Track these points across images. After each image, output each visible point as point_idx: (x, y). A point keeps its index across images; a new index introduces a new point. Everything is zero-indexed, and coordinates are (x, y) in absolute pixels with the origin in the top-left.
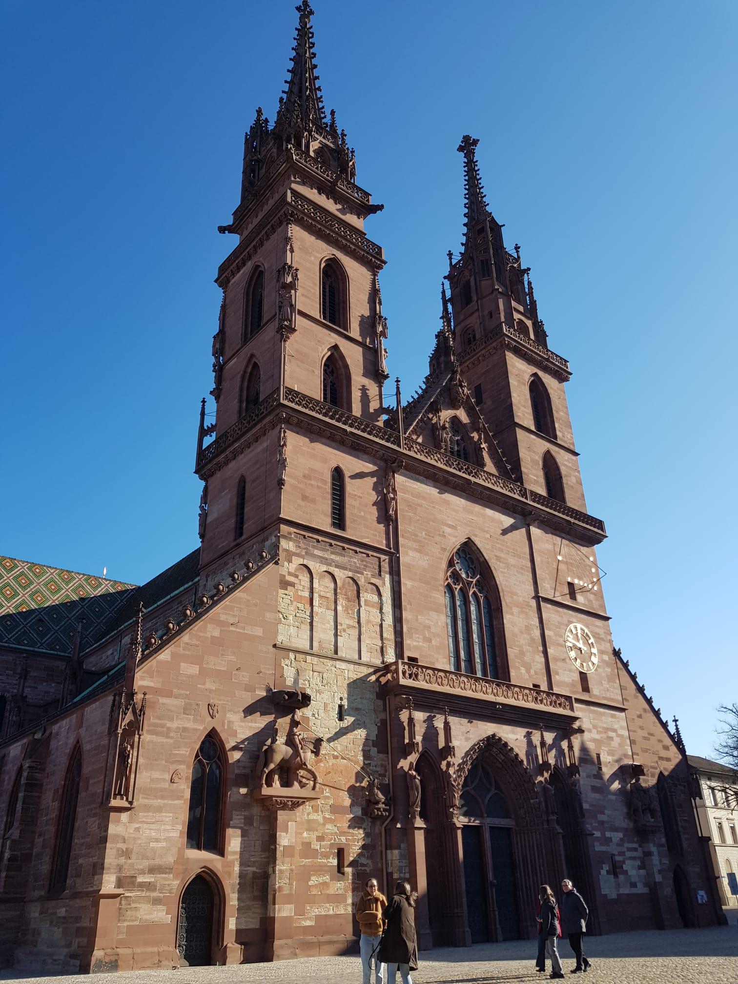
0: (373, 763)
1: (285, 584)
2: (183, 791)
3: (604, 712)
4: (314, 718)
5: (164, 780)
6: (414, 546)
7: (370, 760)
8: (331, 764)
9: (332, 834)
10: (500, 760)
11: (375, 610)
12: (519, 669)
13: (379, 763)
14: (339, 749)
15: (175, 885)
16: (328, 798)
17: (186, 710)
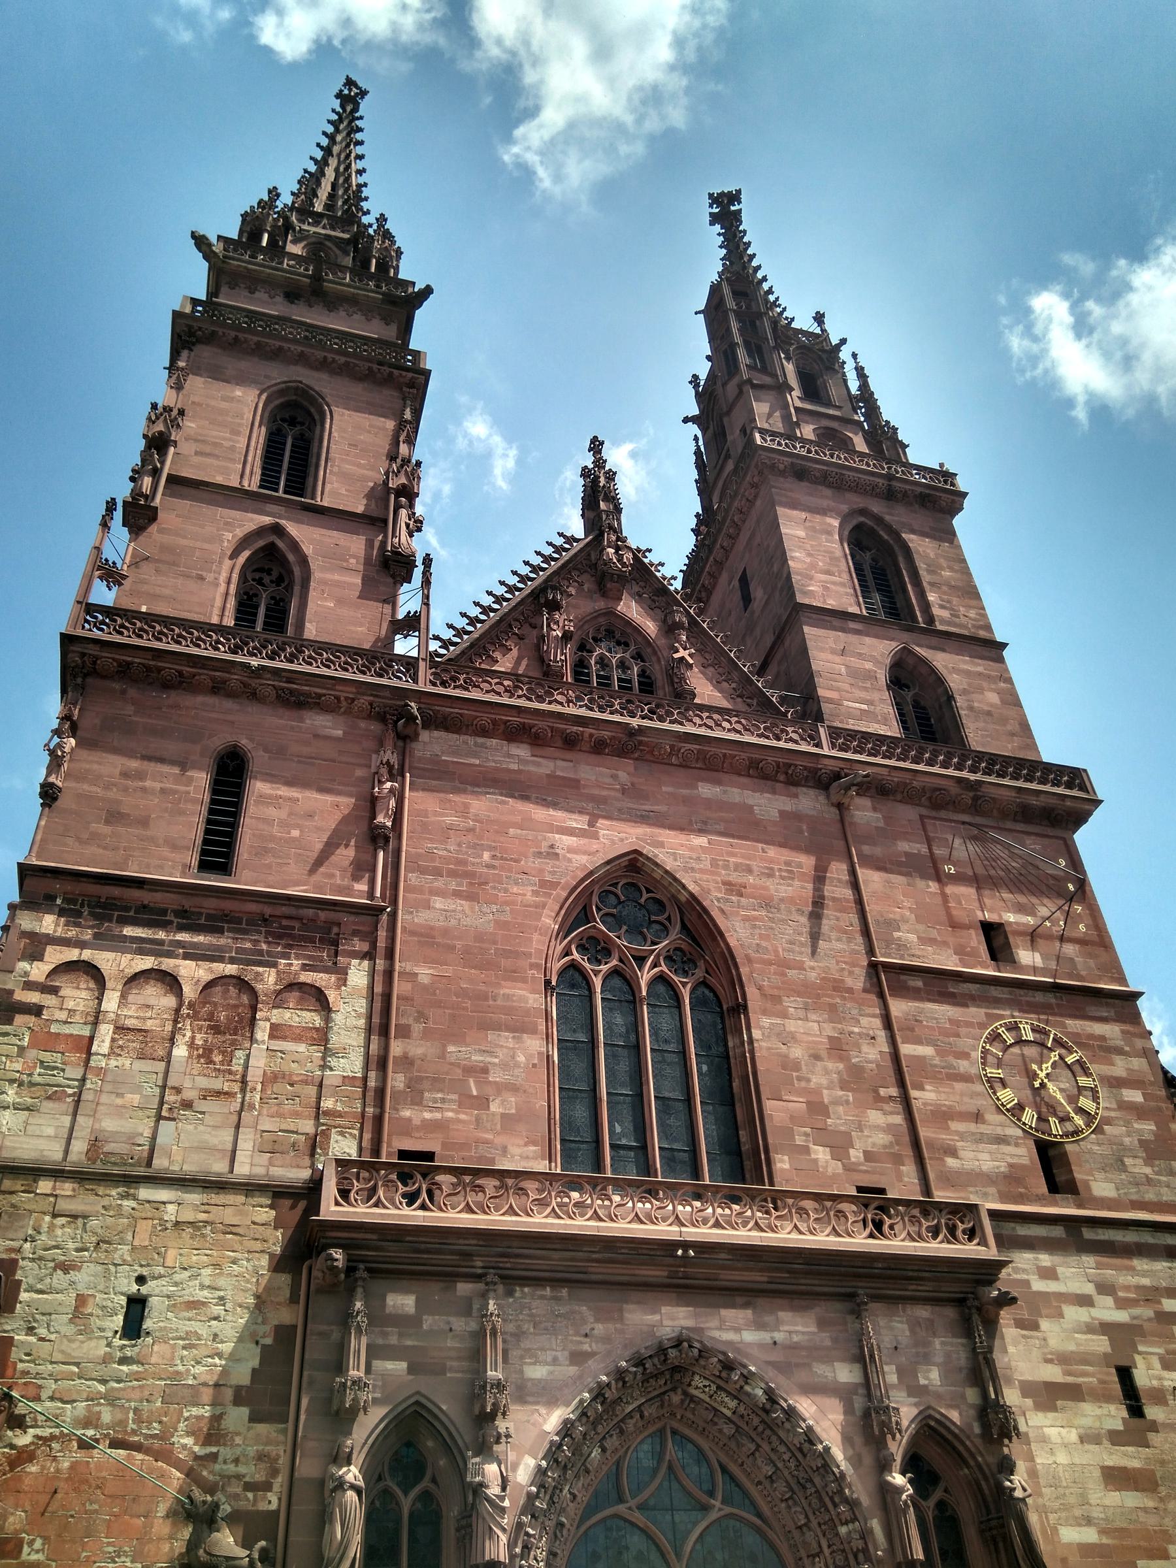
0: (225, 1452)
4: (33, 1339)
6: (453, 886)
7: (217, 1444)
8: (66, 1465)
10: (725, 1411)
11: (302, 1048)
12: (806, 1150)
13: (252, 1451)
14: (107, 1416)
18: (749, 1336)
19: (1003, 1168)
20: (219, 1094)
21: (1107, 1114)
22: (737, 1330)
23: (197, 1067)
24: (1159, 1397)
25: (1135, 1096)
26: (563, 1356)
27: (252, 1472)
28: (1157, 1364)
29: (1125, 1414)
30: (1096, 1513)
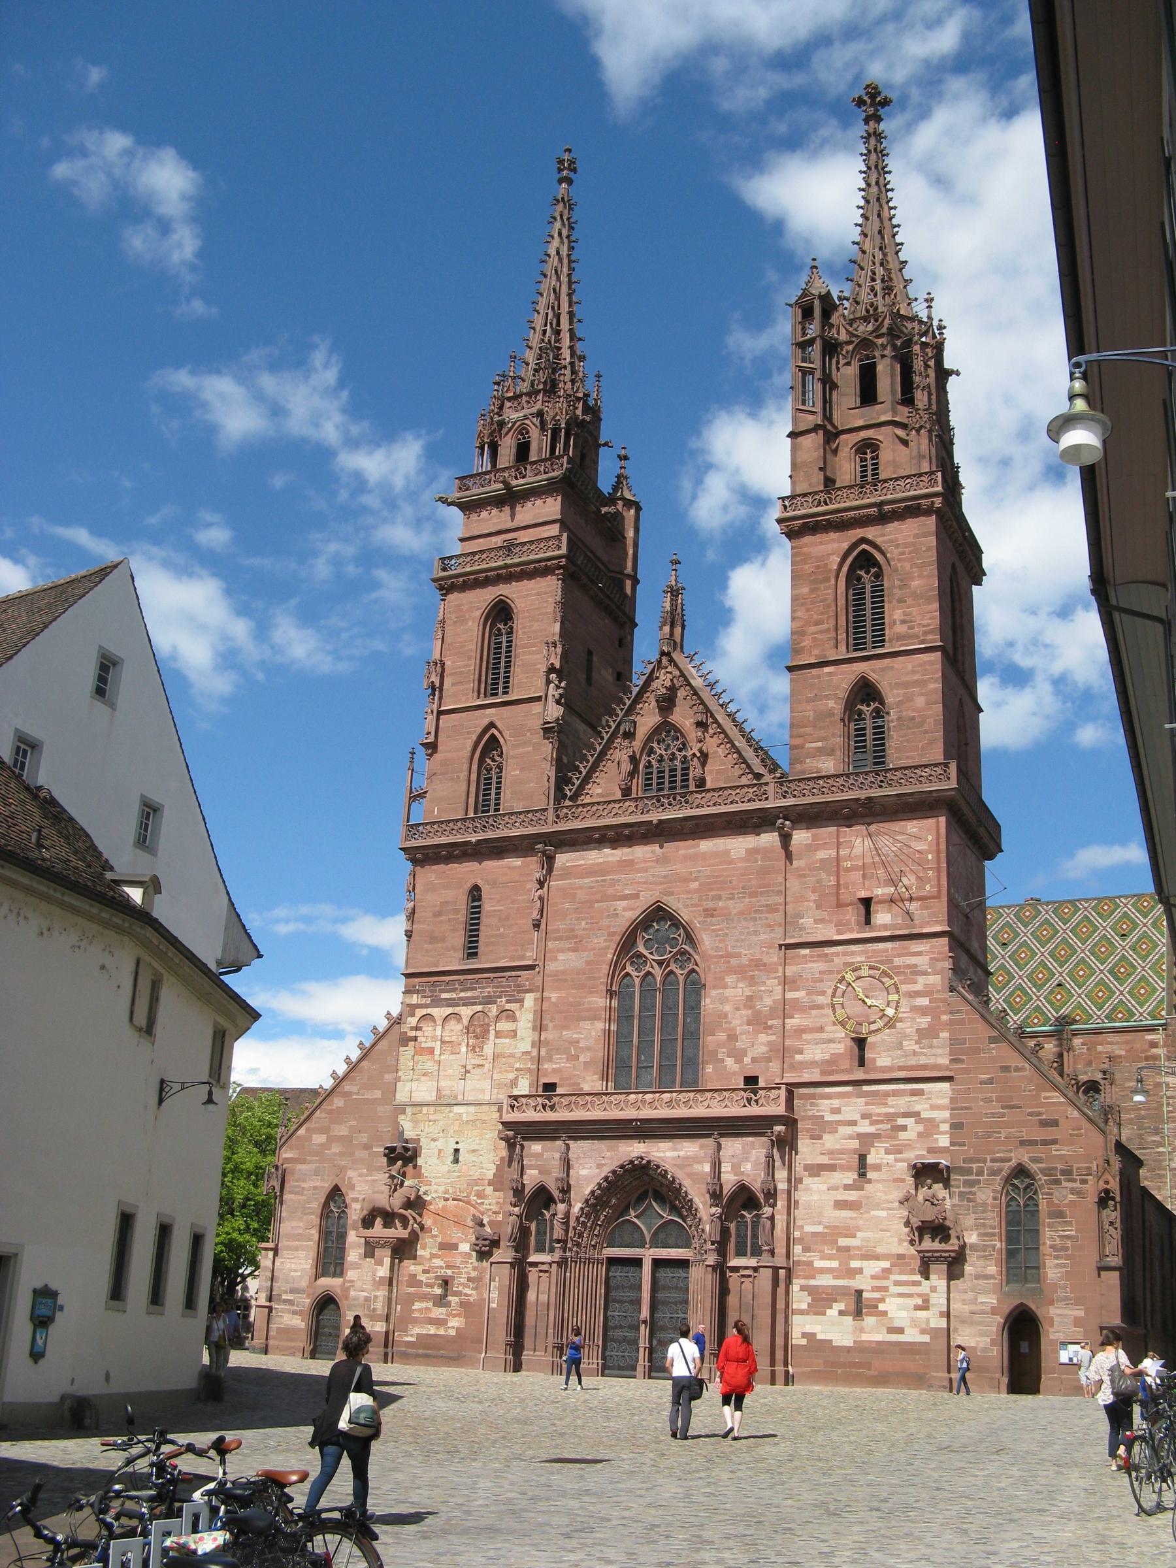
0: (486, 1202)
1: (405, 1040)
2: (312, 1235)
3: (894, 1091)
5: (300, 1227)
9: (437, 1268)
11: (507, 1040)
12: (722, 1060)
14: (451, 1191)
15: (306, 1302)
16: (436, 1236)
17: (317, 1172)
18: (669, 1154)
19: (827, 1056)
20: (479, 1065)
21: (900, 1015)
22: (664, 1152)
23: (469, 1053)
24: (877, 1167)
25: (924, 1001)
26: (594, 1166)
27: (494, 1208)
28: (882, 1151)
29: (856, 1176)
30: (825, 1220)
